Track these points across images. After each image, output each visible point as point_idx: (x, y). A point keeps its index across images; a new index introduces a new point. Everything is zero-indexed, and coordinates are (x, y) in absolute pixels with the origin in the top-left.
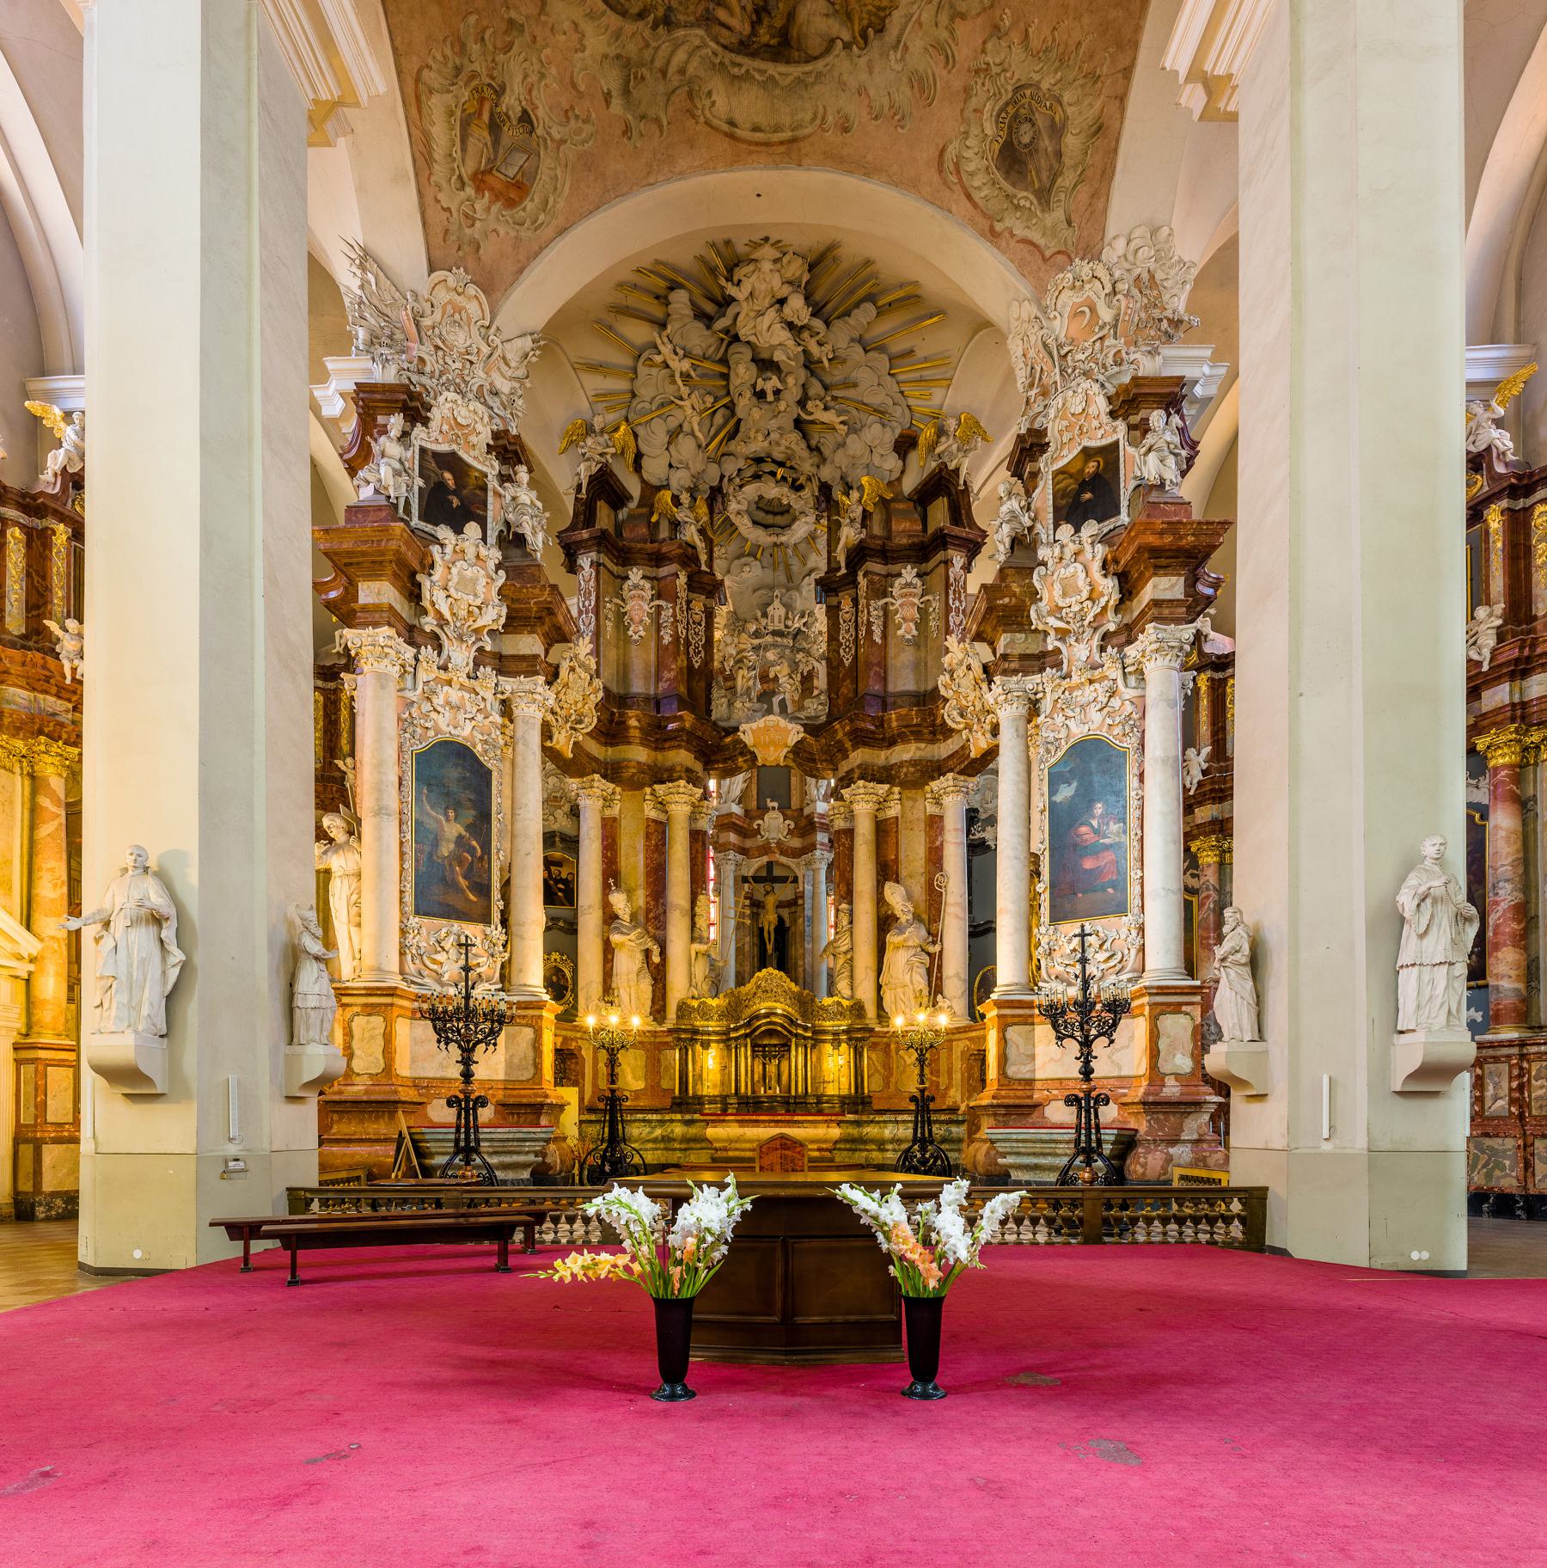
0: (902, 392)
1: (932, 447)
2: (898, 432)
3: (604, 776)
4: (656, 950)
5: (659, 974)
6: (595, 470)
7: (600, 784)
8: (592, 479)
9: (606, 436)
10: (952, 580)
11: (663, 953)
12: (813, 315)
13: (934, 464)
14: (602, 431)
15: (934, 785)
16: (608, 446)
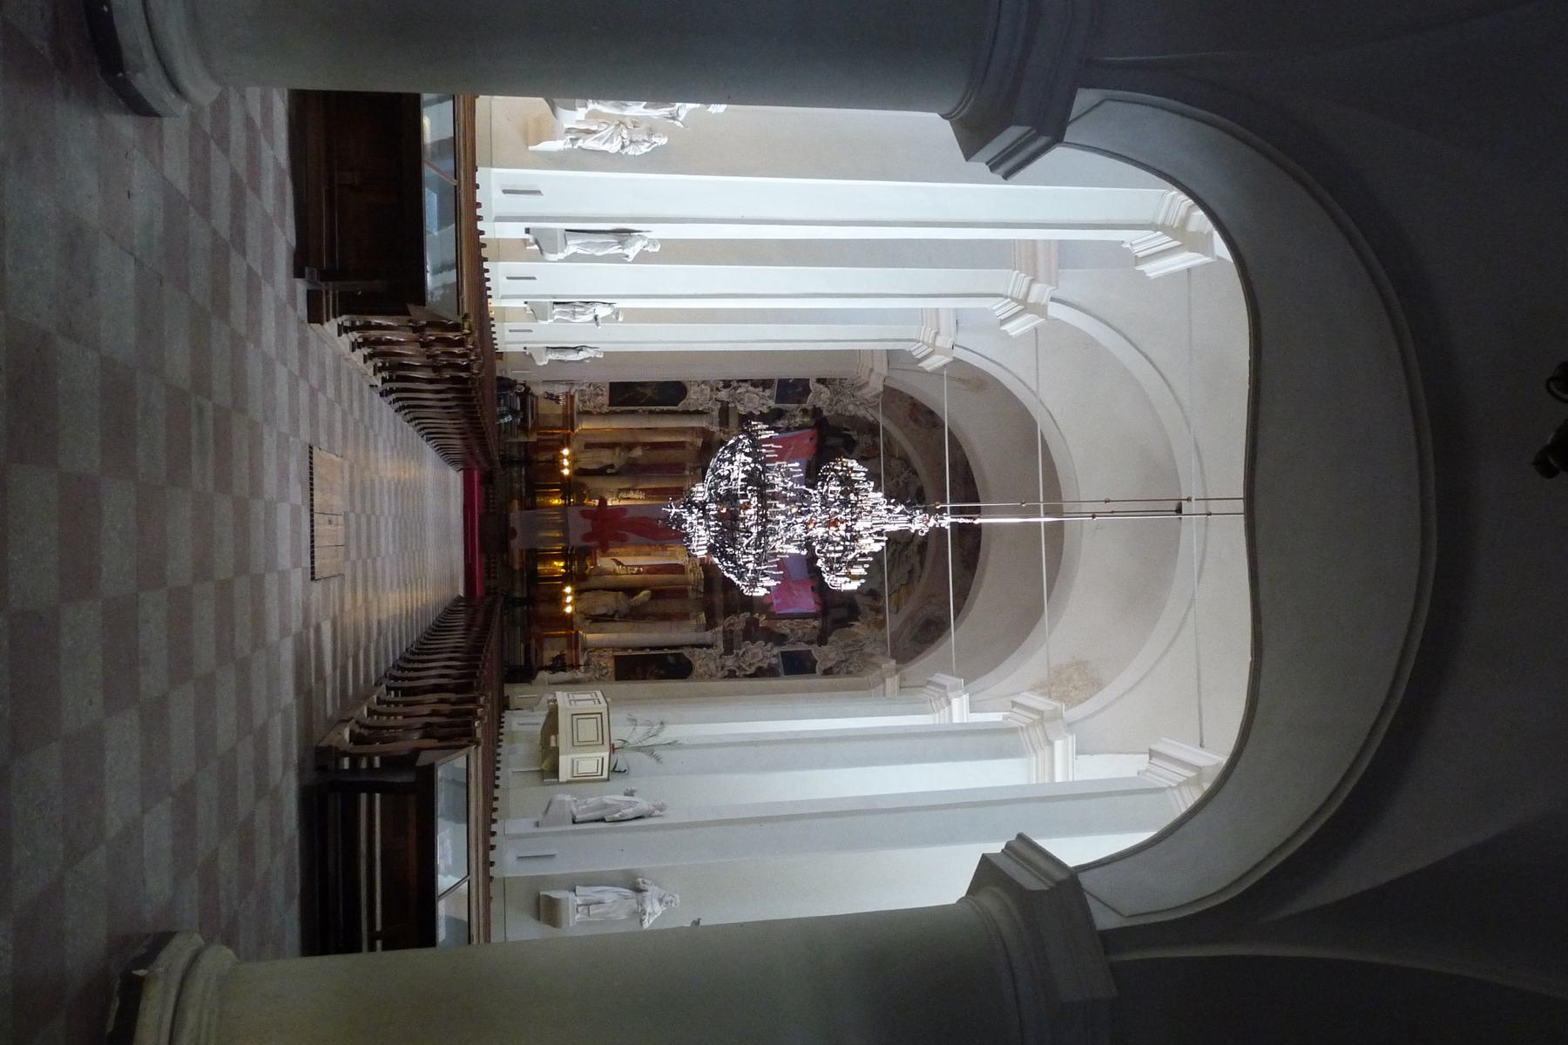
0: (895, 591)
1: (872, 609)
2: (878, 590)
3: (703, 443)
4: (613, 471)
5: (601, 472)
6: (855, 438)
7: (699, 442)
8: (850, 436)
9: (871, 444)
10: (808, 620)
11: (611, 474)
12: (919, 546)
13: (861, 608)
14: (874, 442)
15: (703, 615)
16: (866, 444)
